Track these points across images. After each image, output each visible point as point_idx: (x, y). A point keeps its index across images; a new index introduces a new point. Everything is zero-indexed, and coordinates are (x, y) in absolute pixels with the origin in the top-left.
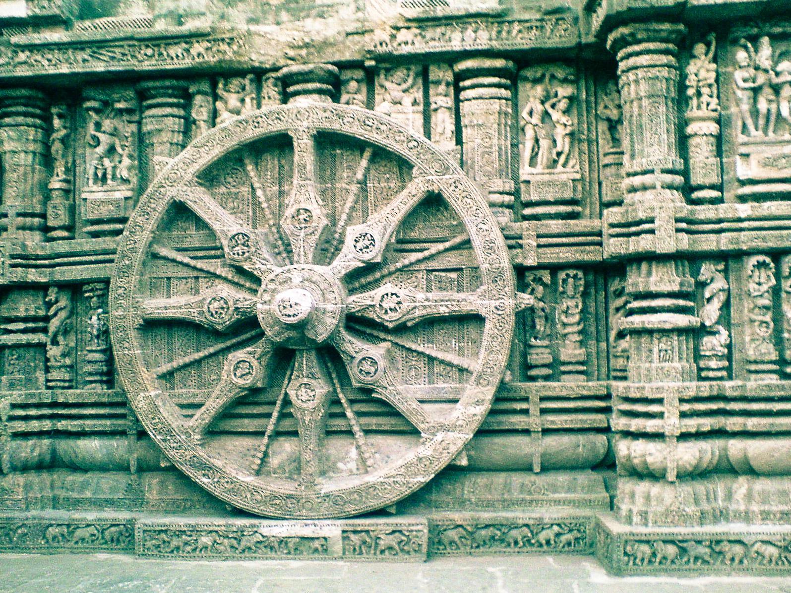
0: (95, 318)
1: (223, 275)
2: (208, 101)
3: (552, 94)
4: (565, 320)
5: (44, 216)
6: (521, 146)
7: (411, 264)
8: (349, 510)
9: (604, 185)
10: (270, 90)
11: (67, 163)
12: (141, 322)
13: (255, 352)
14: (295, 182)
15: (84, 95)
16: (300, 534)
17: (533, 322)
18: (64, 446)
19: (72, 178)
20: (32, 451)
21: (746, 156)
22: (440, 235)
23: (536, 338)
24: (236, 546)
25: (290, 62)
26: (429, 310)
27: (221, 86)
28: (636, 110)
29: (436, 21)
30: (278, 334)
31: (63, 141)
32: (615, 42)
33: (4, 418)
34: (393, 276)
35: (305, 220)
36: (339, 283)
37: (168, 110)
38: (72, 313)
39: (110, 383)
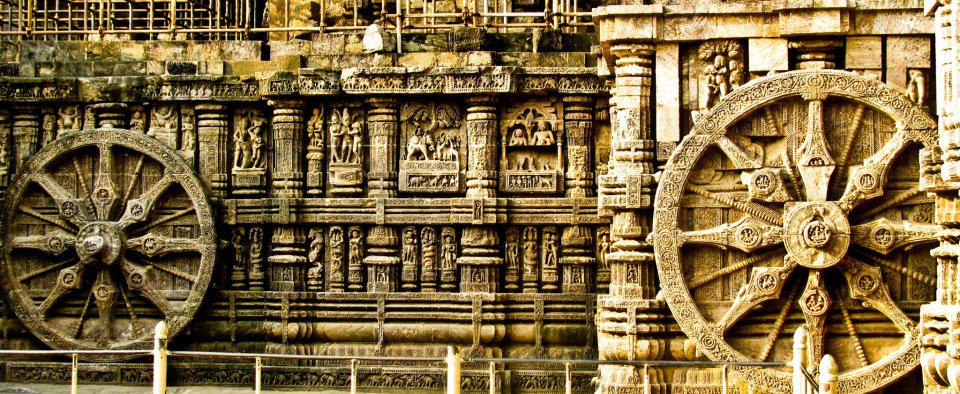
10: (89, 115)
21: (333, 173)
22: (182, 205)
30: (87, 260)
37: (28, 123)
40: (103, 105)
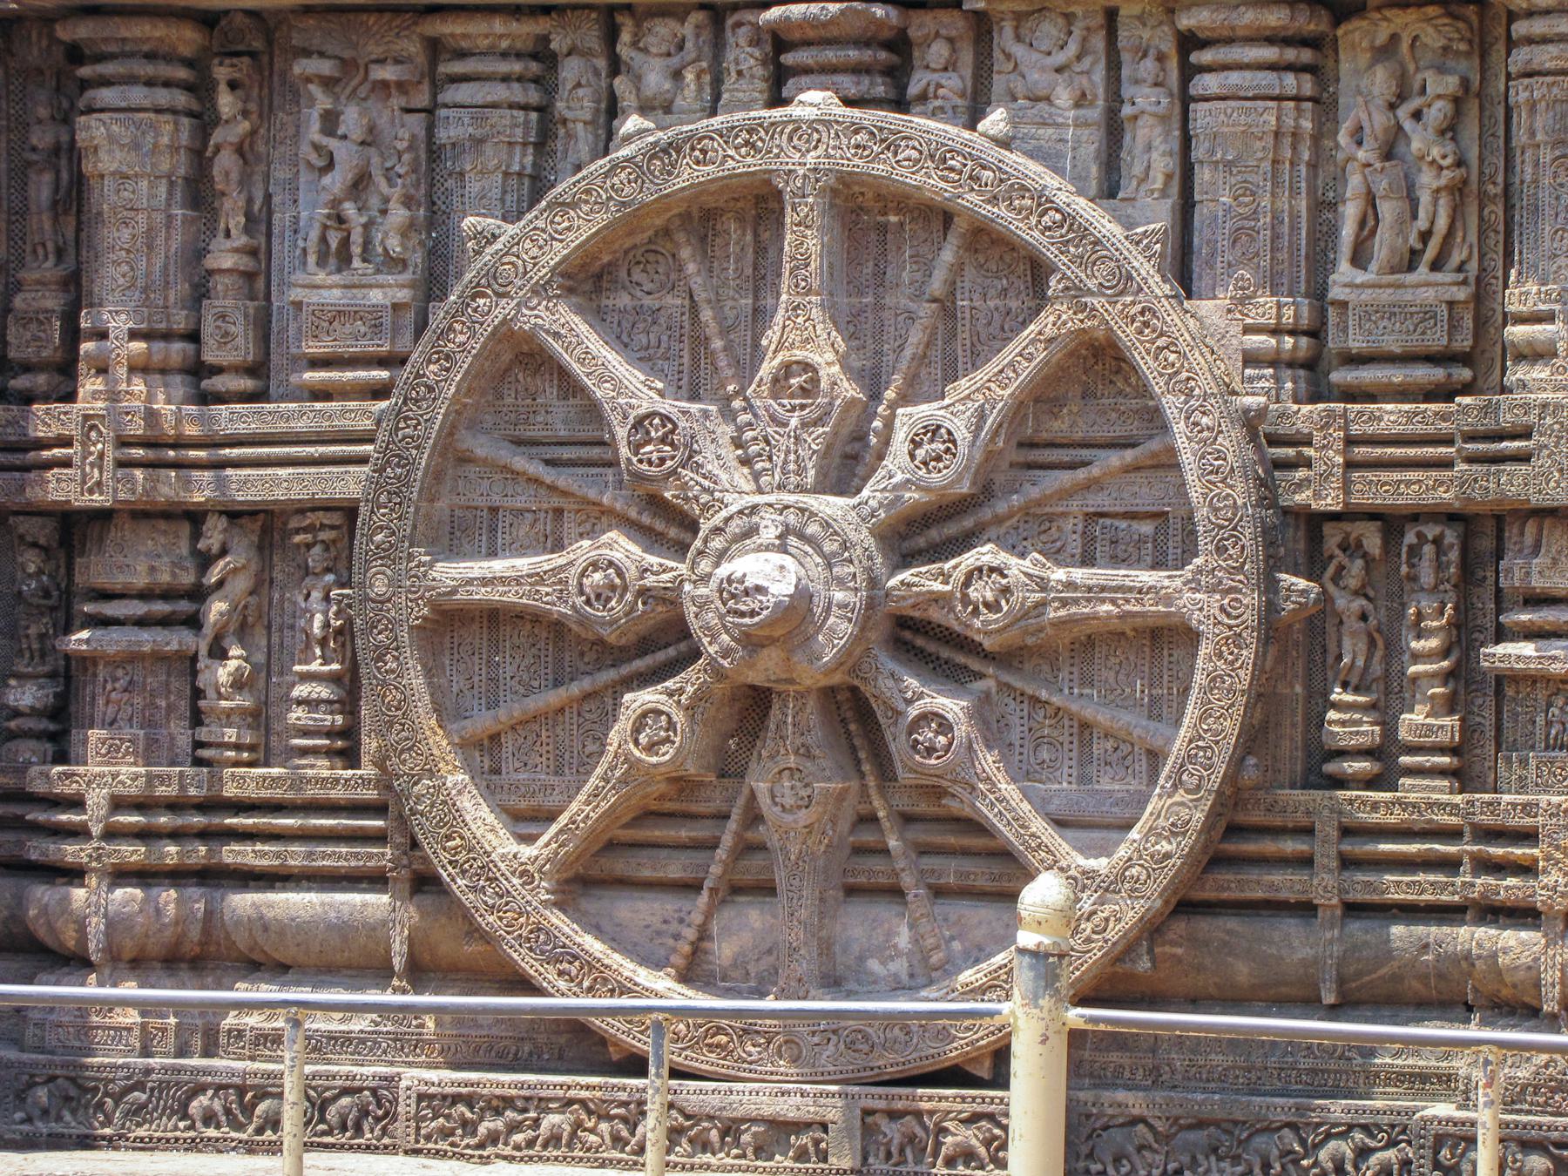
1: (618, 506)
2: (597, 73)
5: (194, 337)
6: (1341, 209)
8: (881, 1063)
10: (744, 56)
11: (250, 201)
12: (425, 611)
13: (681, 691)
14: (784, 297)
17: (1340, 646)
19: (263, 240)
22: (1118, 431)
23: (1345, 686)
24: (625, 1133)
26: (1074, 610)
27: (625, 37)
28: (1529, 170)
33: (96, 830)
34: (1008, 523)
35: (802, 388)
36: (870, 542)
37: (500, 92)
38: (262, 583)
39: (350, 757)
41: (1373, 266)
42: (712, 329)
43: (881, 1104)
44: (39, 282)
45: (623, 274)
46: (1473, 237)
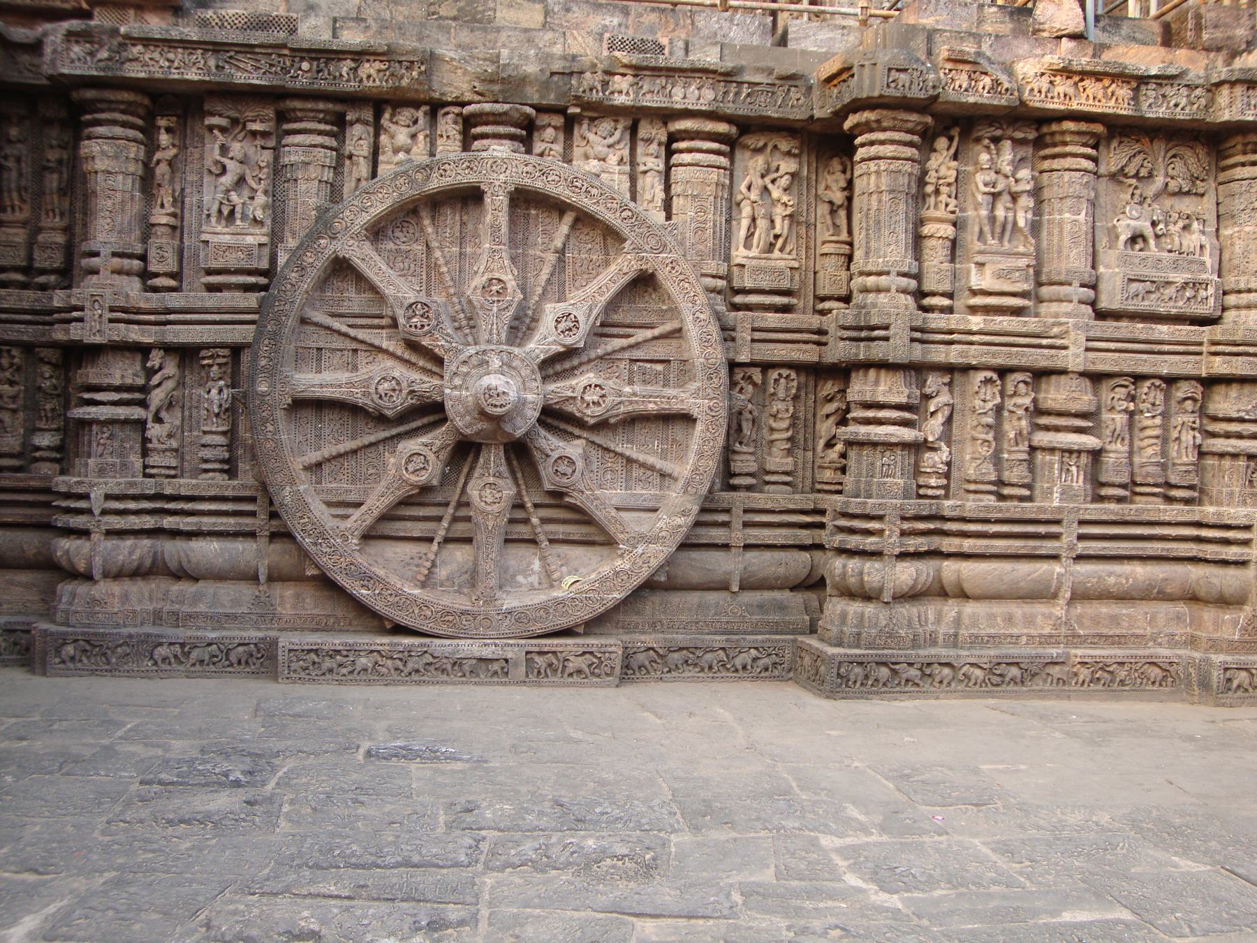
0: (214, 392)
1: (391, 349)
3: (774, 165)
4: (774, 425)
5: (143, 258)
6: (734, 223)
7: (614, 352)
9: (820, 275)
10: (448, 126)
11: (174, 191)
12: (289, 401)
13: (432, 444)
15: (206, 108)
16: (477, 654)
18: (172, 549)
20: (131, 553)
23: (741, 443)
25: (477, 98)
26: (636, 407)
27: (387, 115)
28: (874, 205)
29: (657, 71)
30: (470, 425)
31: (170, 163)
32: (857, 125)
33: (97, 512)
37: (319, 139)
38: (181, 384)
39: (232, 473)
40: (487, 107)
41: (754, 248)
42: (441, 261)
43: (537, 649)
44: (52, 229)
45: (390, 232)
46: (794, 240)
